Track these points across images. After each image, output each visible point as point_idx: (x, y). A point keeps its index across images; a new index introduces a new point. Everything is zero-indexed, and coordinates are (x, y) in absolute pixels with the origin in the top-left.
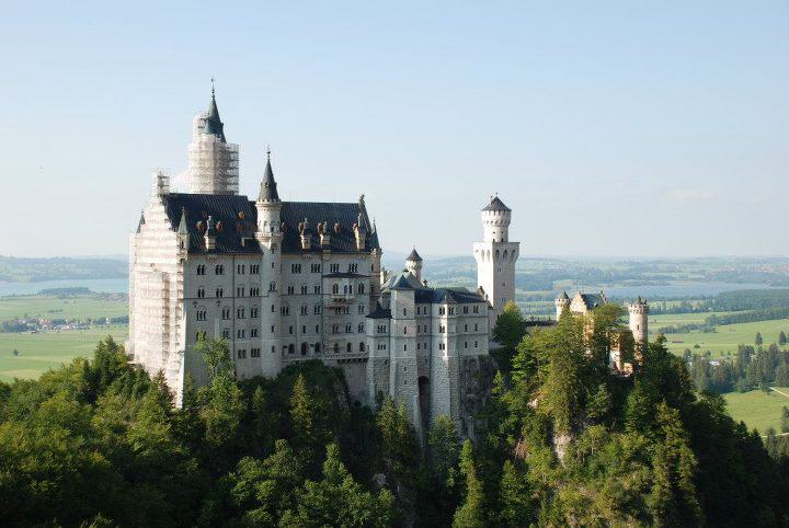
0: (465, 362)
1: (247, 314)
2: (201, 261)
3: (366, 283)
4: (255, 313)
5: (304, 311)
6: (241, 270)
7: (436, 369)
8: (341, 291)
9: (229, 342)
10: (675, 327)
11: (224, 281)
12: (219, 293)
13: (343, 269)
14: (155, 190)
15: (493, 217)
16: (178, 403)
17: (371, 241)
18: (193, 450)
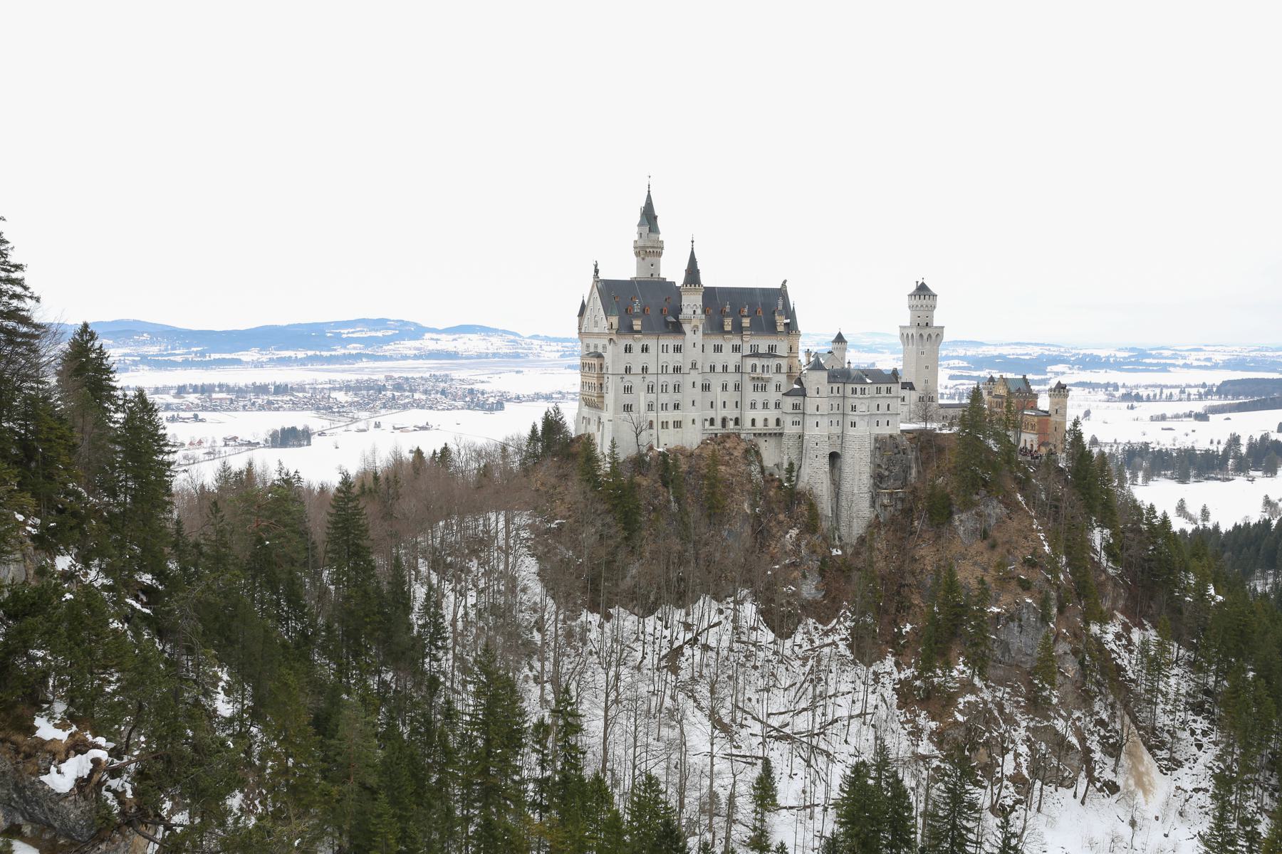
0: (876, 440)
1: (671, 388)
2: (628, 340)
3: (784, 363)
4: (677, 388)
5: (725, 387)
6: (665, 349)
7: (847, 444)
8: (759, 370)
9: (652, 416)
10: (1169, 415)
11: (649, 359)
12: (645, 370)
13: (763, 349)
14: (590, 280)
15: (916, 302)
16: (606, 467)
17: (791, 328)
18: (615, 506)
